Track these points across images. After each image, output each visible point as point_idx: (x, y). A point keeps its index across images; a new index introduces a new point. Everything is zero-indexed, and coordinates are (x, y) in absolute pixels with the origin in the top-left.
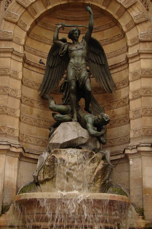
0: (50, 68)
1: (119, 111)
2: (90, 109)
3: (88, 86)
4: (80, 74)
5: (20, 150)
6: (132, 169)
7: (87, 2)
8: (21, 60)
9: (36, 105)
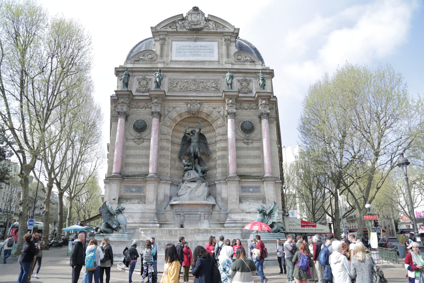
0: (183, 145)
1: (212, 164)
2: (200, 164)
3: (199, 155)
4: (195, 150)
5: (171, 182)
6: (217, 190)
9: (177, 161)
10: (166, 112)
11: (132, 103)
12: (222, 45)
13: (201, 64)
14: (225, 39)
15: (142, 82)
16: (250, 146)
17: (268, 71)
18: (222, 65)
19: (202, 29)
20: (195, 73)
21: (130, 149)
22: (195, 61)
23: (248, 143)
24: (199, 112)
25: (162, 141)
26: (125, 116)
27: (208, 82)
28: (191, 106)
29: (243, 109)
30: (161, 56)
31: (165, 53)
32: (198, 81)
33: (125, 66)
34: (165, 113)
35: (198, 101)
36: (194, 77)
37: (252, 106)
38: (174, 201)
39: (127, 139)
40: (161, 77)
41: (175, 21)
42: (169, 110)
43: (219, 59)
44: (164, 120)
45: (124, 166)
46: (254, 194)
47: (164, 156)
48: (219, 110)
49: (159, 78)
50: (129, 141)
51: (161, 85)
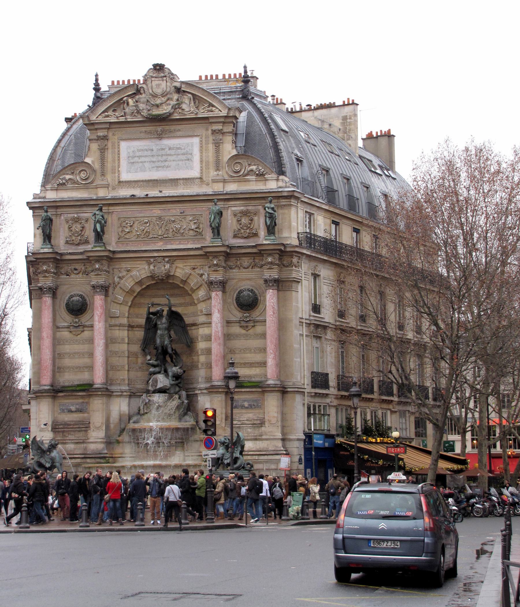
3: (170, 350)
4: (164, 342)
5: (129, 394)
7: (171, 281)
8: (126, 328)
9: (140, 356)
10: (116, 279)
11: (61, 266)
12: (207, 143)
13: (172, 186)
14: (212, 130)
15: (74, 227)
16: (251, 331)
17: (285, 194)
18: (208, 184)
19: (170, 114)
20: (160, 204)
21: (64, 344)
22: (160, 180)
23: (247, 326)
24: (168, 276)
25: (113, 328)
26: (52, 292)
27: (183, 220)
28: (156, 268)
29: (242, 268)
30: (103, 174)
31: (109, 165)
32: (166, 218)
33: (43, 195)
34: (114, 281)
35: (167, 259)
36: (159, 212)
37: (257, 261)
38: (134, 423)
39: (58, 328)
40: (103, 222)
41: (122, 99)
42: (120, 275)
43: (202, 173)
44: (115, 292)
45: (56, 370)
46: (250, 411)
47: (116, 353)
48: (201, 272)
49: (100, 222)
50: (61, 330)
51: (104, 233)
